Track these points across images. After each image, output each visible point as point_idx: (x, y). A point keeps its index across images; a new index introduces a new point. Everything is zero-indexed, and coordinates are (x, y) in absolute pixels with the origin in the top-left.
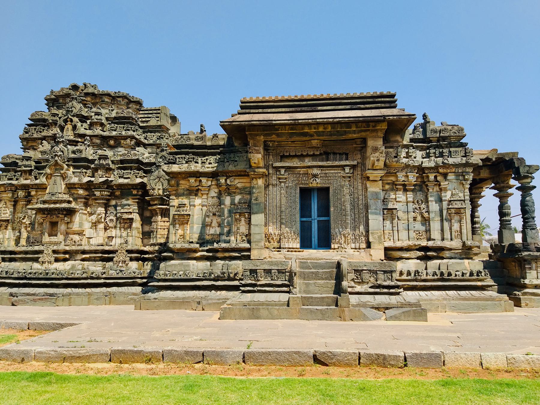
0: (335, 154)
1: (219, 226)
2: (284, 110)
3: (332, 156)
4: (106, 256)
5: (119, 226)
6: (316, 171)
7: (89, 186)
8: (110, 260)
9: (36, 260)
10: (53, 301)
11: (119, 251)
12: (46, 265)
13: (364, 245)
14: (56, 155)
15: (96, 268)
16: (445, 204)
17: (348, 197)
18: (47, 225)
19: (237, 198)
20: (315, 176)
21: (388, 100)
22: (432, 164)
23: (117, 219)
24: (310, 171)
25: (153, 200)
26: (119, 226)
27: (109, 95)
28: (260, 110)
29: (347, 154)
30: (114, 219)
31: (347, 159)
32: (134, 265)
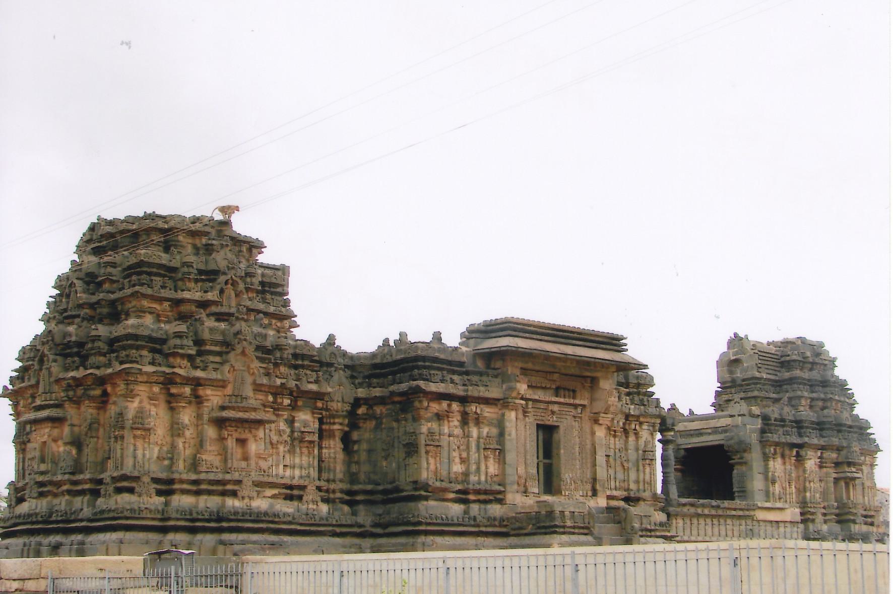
0: (565, 389)
1: (463, 461)
2: (546, 338)
3: (562, 392)
4: (293, 492)
5: (298, 450)
6: (556, 408)
7: (277, 392)
8: (300, 498)
9: (234, 494)
10: (287, 550)
11: (309, 488)
12: (246, 500)
13: (590, 493)
14: (245, 340)
15: (286, 508)
16: (640, 452)
17: (577, 440)
18: (231, 443)
19: (485, 430)
20: (553, 413)
21: (613, 342)
22: (637, 413)
23: (293, 440)
24: (551, 407)
25: (334, 417)
26: (298, 450)
27: (248, 242)
28: (527, 335)
29: (574, 391)
30: (288, 439)
31: (574, 398)
32: (324, 508)
